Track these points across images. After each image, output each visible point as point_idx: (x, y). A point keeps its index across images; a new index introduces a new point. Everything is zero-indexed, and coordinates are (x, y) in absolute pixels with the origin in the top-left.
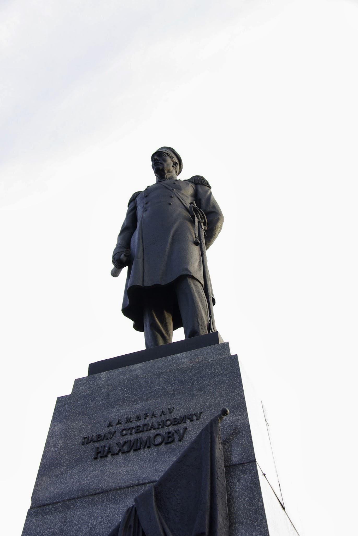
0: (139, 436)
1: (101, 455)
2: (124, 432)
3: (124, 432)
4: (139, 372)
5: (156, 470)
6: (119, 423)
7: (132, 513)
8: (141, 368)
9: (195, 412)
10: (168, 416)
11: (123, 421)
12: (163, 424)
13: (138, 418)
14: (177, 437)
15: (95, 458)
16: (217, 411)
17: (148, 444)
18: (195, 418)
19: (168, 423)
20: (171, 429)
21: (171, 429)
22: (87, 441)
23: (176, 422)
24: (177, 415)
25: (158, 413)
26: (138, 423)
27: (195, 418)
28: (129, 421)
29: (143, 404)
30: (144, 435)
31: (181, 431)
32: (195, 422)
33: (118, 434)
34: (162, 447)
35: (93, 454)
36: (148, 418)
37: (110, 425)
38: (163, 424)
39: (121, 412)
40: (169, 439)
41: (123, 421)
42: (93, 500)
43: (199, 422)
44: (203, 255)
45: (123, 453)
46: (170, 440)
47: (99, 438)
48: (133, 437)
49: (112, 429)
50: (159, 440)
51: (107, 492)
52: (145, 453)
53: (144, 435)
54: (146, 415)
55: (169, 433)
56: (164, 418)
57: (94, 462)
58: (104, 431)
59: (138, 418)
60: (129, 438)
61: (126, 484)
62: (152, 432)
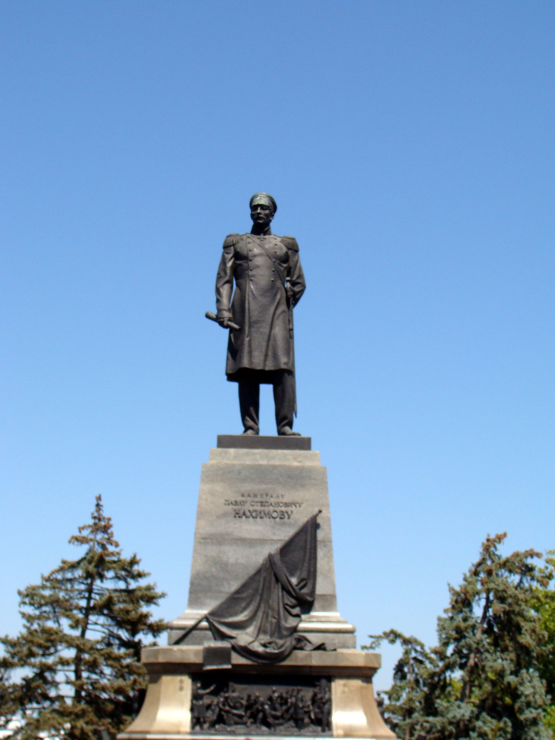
0: (263, 508)
1: (238, 515)
2: (253, 503)
3: (253, 503)
6: (249, 496)
10: (280, 500)
11: (252, 495)
16: (316, 510)
17: (269, 515)
18: (298, 505)
20: (283, 509)
23: (286, 505)
24: (286, 500)
25: (274, 496)
26: (262, 500)
27: (298, 505)
29: (264, 487)
30: (266, 509)
32: (298, 508)
33: (248, 504)
34: (278, 519)
35: (233, 513)
36: (268, 497)
37: (243, 495)
38: (278, 504)
41: (252, 495)
43: (302, 508)
44: (290, 321)
45: (253, 517)
47: (236, 503)
48: (258, 508)
49: (243, 499)
52: (266, 520)
54: (267, 495)
55: (282, 512)
57: (234, 519)
58: (239, 499)
59: (262, 495)
60: (256, 508)
62: (271, 509)
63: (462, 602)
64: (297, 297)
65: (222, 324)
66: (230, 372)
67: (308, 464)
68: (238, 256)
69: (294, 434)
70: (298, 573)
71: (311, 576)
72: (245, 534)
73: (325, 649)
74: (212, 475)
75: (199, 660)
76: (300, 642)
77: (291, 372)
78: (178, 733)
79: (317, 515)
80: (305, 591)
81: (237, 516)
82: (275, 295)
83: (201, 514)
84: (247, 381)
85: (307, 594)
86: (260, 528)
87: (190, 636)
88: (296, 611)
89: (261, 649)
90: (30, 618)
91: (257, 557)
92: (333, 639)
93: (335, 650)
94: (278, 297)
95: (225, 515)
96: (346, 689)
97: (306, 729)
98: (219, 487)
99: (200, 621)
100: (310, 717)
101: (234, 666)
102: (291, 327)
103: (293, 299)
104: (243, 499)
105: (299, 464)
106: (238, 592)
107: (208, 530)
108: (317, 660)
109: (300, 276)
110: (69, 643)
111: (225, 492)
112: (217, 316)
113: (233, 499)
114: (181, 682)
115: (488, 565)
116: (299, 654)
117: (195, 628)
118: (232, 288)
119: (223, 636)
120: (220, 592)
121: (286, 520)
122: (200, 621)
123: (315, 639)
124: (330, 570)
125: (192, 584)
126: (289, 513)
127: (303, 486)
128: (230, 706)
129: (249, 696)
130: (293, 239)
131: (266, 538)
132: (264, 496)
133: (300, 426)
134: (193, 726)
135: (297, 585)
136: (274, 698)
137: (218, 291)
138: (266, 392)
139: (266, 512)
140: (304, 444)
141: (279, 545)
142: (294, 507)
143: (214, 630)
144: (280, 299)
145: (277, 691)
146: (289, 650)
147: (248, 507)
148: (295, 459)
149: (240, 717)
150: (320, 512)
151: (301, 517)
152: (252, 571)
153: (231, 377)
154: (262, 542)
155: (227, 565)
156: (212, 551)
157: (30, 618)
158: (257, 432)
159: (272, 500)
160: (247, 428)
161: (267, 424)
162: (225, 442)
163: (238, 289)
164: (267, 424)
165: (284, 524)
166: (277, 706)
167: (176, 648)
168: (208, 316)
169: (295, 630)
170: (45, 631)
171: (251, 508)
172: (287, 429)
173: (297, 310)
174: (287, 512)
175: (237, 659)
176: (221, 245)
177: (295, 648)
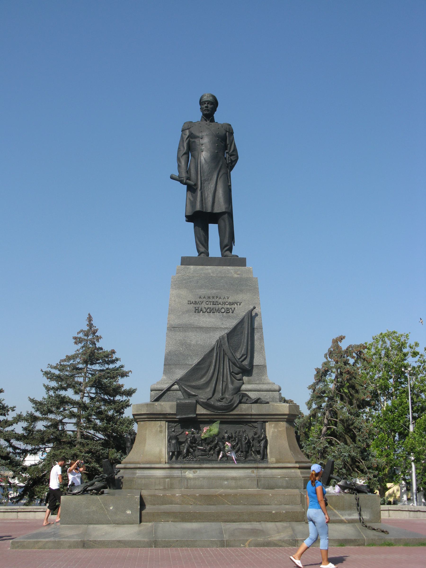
0: (214, 306)
1: (198, 311)
4: (210, 271)
5: (222, 323)
7: (219, 343)
8: (210, 269)
9: (238, 301)
11: (206, 297)
12: (224, 303)
13: (213, 297)
14: (231, 311)
15: (195, 312)
17: (219, 311)
18: (238, 304)
19: (227, 303)
20: (228, 306)
21: (228, 306)
22: (190, 303)
23: (231, 304)
24: (230, 300)
25: (222, 297)
26: (213, 300)
28: (209, 298)
29: (215, 291)
30: (217, 307)
31: (233, 309)
33: (204, 303)
34: (225, 314)
37: (200, 298)
38: (224, 303)
39: (205, 293)
40: (227, 311)
41: (206, 297)
42: (196, 330)
43: (241, 306)
46: (228, 311)
47: (196, 303)
48: (212, 306)
49: (200, 300)
50: (223, 310)
51: (202, 328)
52: (217, 314)
53: (217, 307)
54: (217, 297)
56: (224, 300)
58: (198, 300)
59: (213, 297)
60: (209, 306)
61: (210, 326)
63: (321, 375)
64: (233, 164)
65: (181, 182)
66: (187, 214)
67: (245, 276)
68: (192, 136)
69: (234, 256)
70: (240, 350)
71: (251, 351)
72: (202, 324)
73: (261, 403)
74: (181, 283)
75: (174, 411)
76: (244, 398)
77: (230, 214)
78: (160, 463)
79: (252, 310)
80: (246, 363)
81: (197, 311)
82: (219, 162)
83: (172, 311)
84: (200, 219)
85: (246, 365)
86: (213, 320)
87: (166, 394)
88: (239, 376)
90: (48, 389)
91: (212, 339)
92: (266, 396)
93: (268, 403)
94: (221, 163)
95: (188, 311)
96: (276, 430)
98: (183, 292)
99: (173, 385)
101: (197, 415)
102: (229, 184)
103: (231, 165)
104: (200, 300)
105: (239, 276)
106: (199, 364)
107: (176, 322)
108: (255, 409)
109: (235, 150)
110: (74, 403)
111: (186, 295)
112: (179, 176)
113: (193, 300)
115: (336, 352)
116: (244, 406)
117: (169, 389)
118: (188, 157)
119: (190, 396)
120: (186, 364)
121: (231, 314)
122: (173, 385)
123: (253, 395)
124: (262, 348)
125: (166, 359)
126: (233, 309)
127: (241, 291)
130: (230, 125)
131: (220, 325)
132: (215, 298)
133: (237, 250)
134: (170, 458)
135: (239, 359)
137: (179, 160)
138: (213, 229)
139: (217, 309)
140: (242, 262)
141: (227, 331)
142: (236, 305)
143: (183, 391)
144: (222, 165)
147: (204, 305)
148: (236, 273)
150: (254, 308)
151: (241, 312)
152: (207, 350)
153: (189, 218)
154: (215, 329)
155: (190, 345)
156: (179, 336)
157: (48, 389)
158: (208, 255)
159: (220, 301)
160: (200, 253)
161: (215, 250)
162: (186, 261)
163: (193, 158)
164: (215, 250)
165: (229, 317)
167: (156, 403)
168: (172, 178)
169: (238, 390)
170: (58, 396)
171: (206, 306)
172: (228, 253)
173: (233, 173)
174: (231, 308)
175: (200, 410)
176: (181, 130)
177: (240, 402)
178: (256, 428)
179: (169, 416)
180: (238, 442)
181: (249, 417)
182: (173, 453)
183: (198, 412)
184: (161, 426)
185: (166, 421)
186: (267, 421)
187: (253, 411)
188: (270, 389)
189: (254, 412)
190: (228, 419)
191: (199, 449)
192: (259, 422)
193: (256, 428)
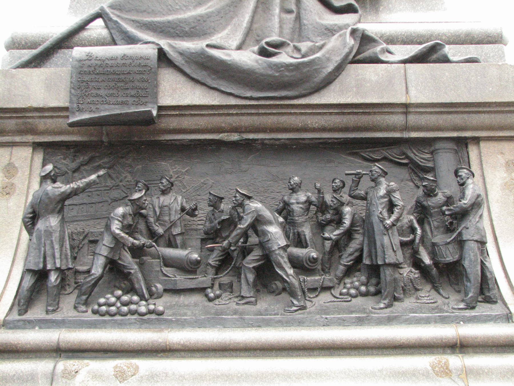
89: (248, 58)
97: (409, 303)
100: (417, 264)
108: (424, 86)
114: (10, 170)
128: (152, 234)
129: (216, 202)
136: (296, 208)
145: (308, 182)
146: (337, 59)
149: (189, 268)
166: (307, 231)
178: (427, 170)
179: (42, 124)
180: (352, 224)
181: (397, 119)
182: (41, 276)
183: (166, 100)
184: (10, 170)
185: (36, 146)
186: (477, 140)
187: (413, 92)
188: (468, 35)
189: (417, 96)
190: (305, 129)
191: (168, 262)
192: (439, 145)
193: (427, 170)
